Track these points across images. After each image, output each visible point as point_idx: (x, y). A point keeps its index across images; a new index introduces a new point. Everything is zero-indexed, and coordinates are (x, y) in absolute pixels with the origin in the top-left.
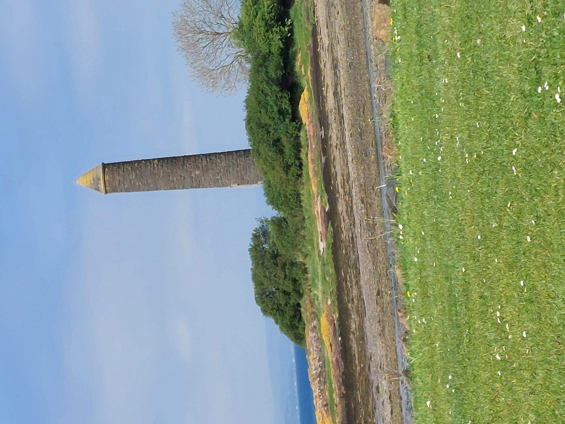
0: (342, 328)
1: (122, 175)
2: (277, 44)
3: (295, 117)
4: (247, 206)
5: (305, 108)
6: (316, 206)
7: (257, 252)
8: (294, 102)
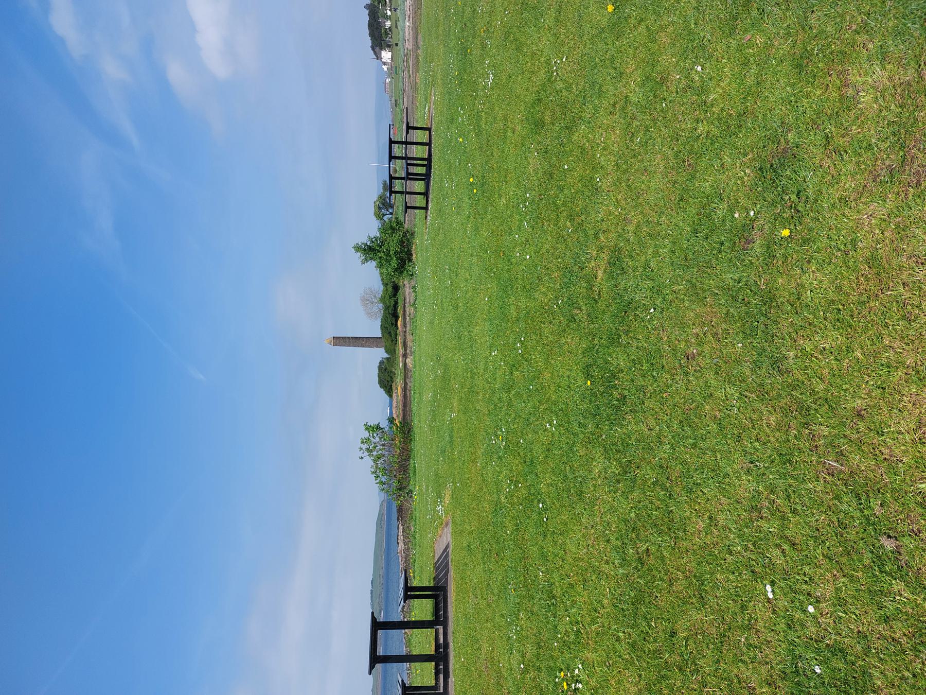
0: (405, 389)
1: (339, 341)
2: (393, 303)
3: (396, 325)
4: (379, 354)
5: (399, 323)
6: (400, 352)
7: (380, 368)
8: (396, 321)
